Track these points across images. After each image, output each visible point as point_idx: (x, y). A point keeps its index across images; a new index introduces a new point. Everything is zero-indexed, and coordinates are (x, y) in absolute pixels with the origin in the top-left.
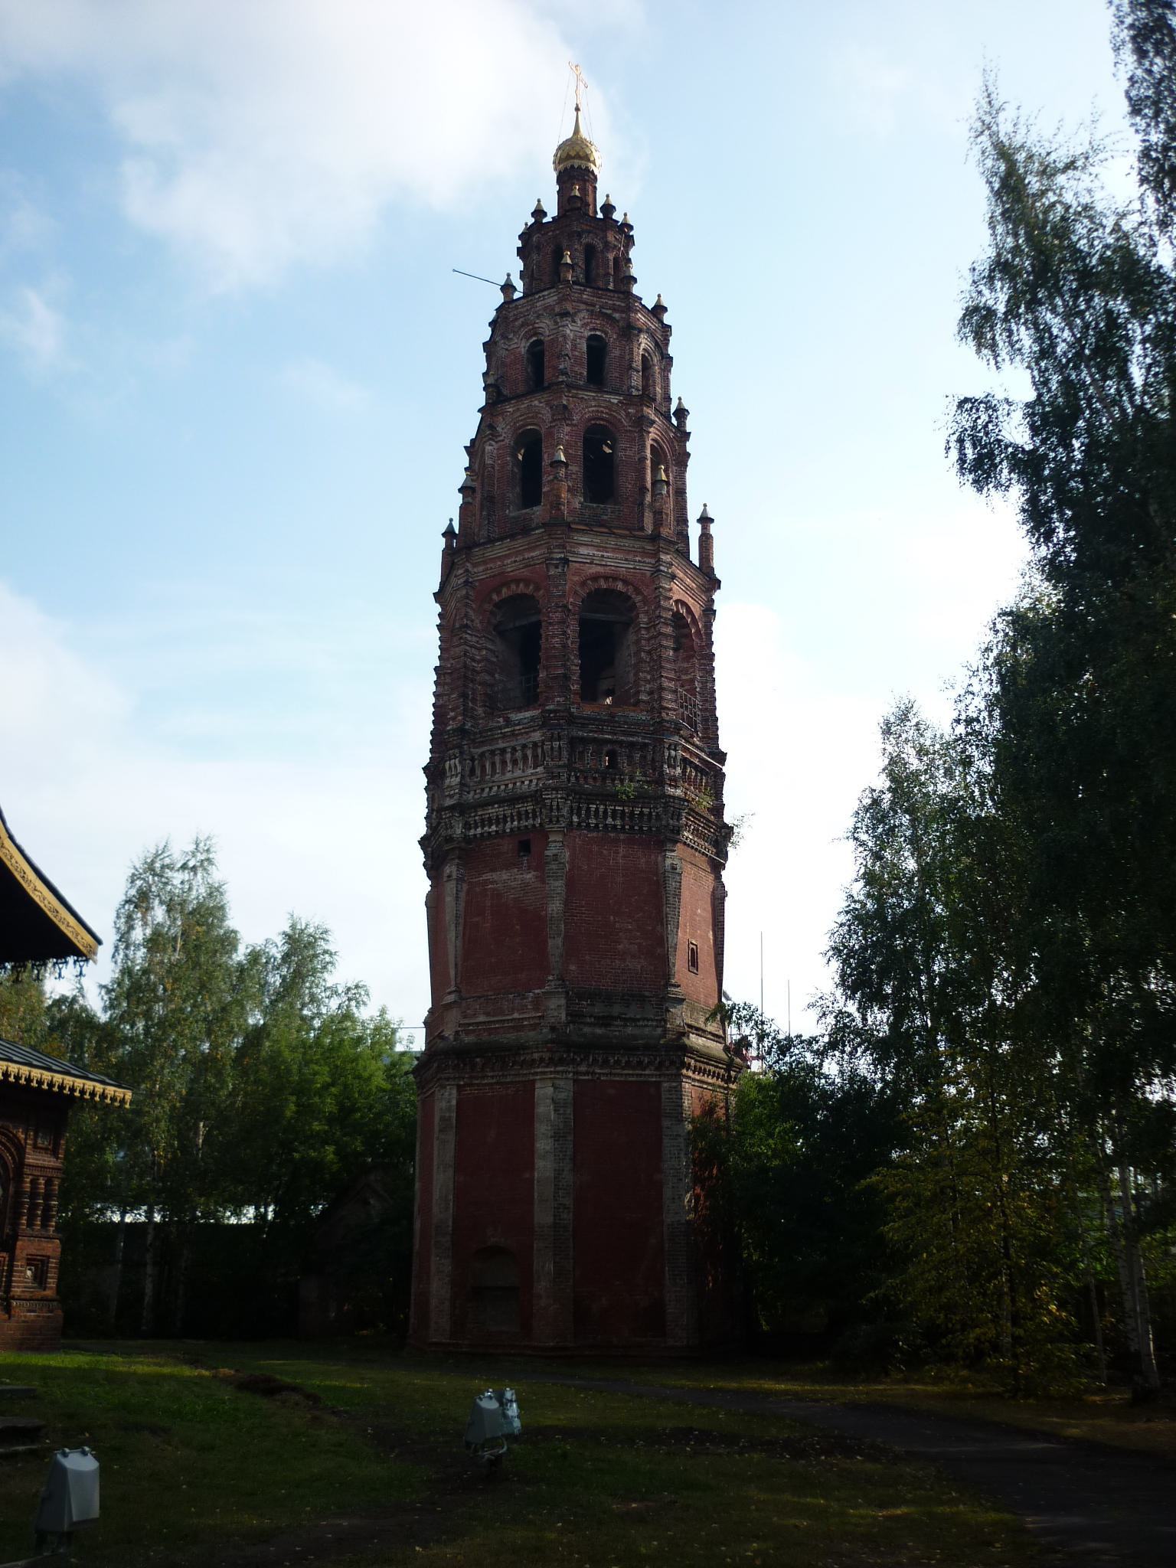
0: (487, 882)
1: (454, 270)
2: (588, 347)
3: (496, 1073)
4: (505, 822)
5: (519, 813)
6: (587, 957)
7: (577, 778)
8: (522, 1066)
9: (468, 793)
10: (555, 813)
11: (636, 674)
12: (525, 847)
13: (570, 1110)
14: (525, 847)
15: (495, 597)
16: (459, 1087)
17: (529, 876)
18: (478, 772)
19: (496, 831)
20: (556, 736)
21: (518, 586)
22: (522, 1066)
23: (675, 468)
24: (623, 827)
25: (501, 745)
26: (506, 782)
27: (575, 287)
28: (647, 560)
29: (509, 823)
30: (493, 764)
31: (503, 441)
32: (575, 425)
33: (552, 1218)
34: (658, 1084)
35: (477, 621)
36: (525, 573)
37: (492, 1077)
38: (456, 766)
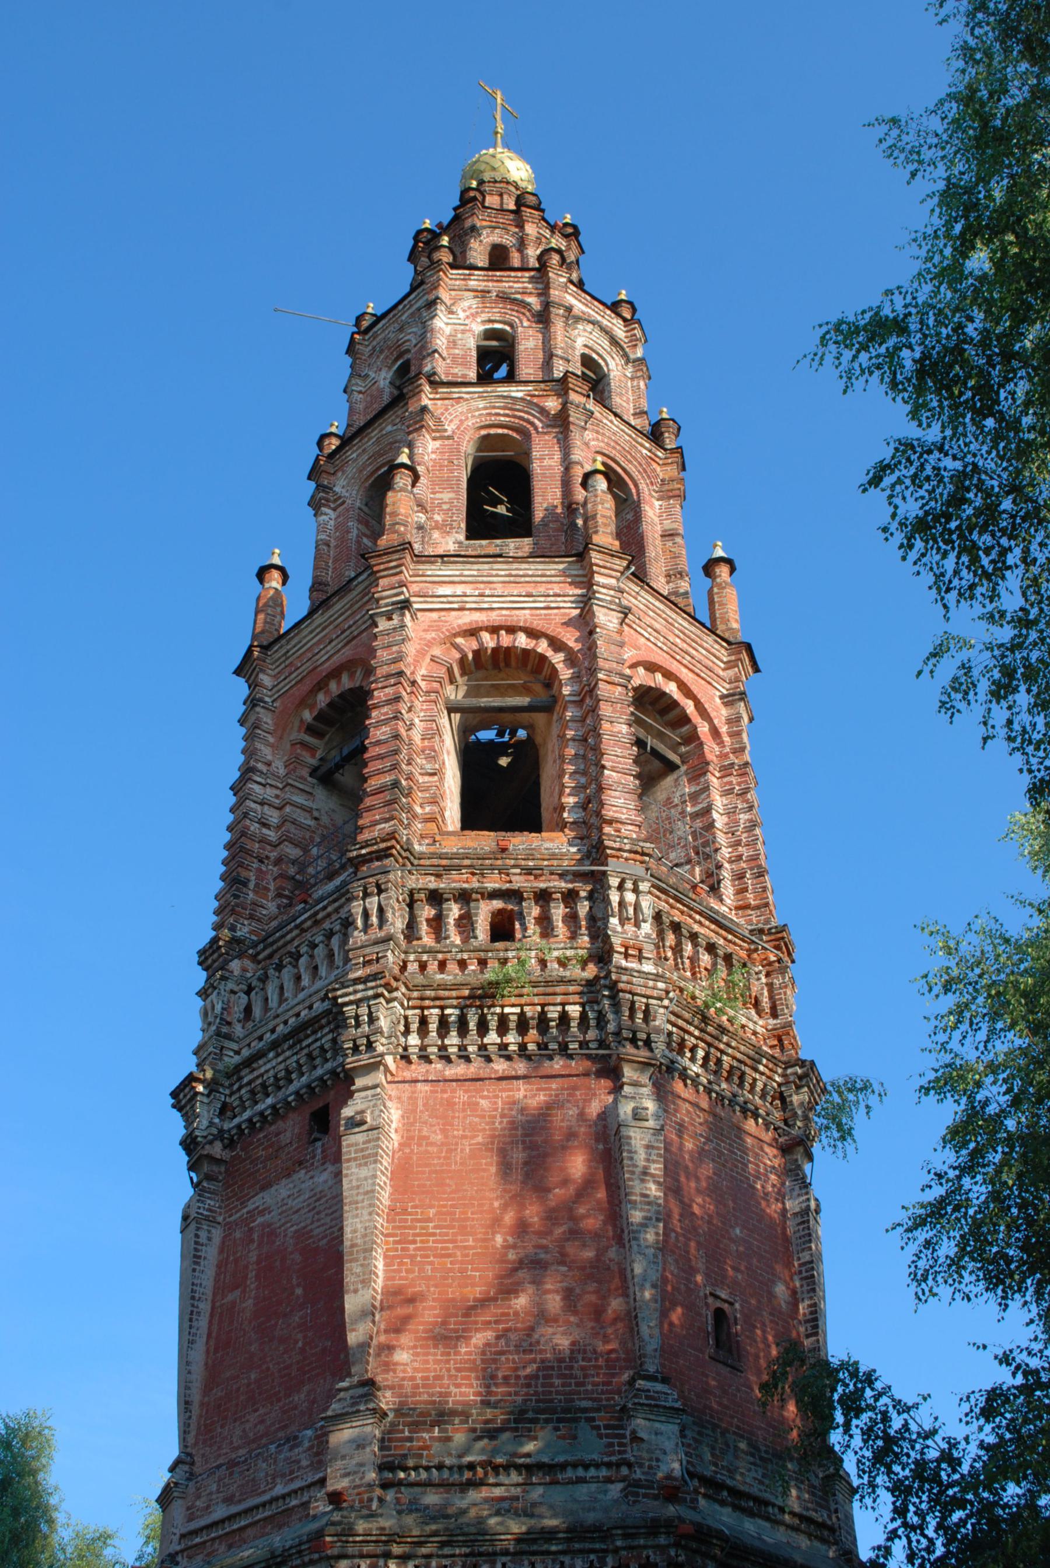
23: (657, 504)
24: (523, 1047)
26: (296, 1010)
32: (449, 438)
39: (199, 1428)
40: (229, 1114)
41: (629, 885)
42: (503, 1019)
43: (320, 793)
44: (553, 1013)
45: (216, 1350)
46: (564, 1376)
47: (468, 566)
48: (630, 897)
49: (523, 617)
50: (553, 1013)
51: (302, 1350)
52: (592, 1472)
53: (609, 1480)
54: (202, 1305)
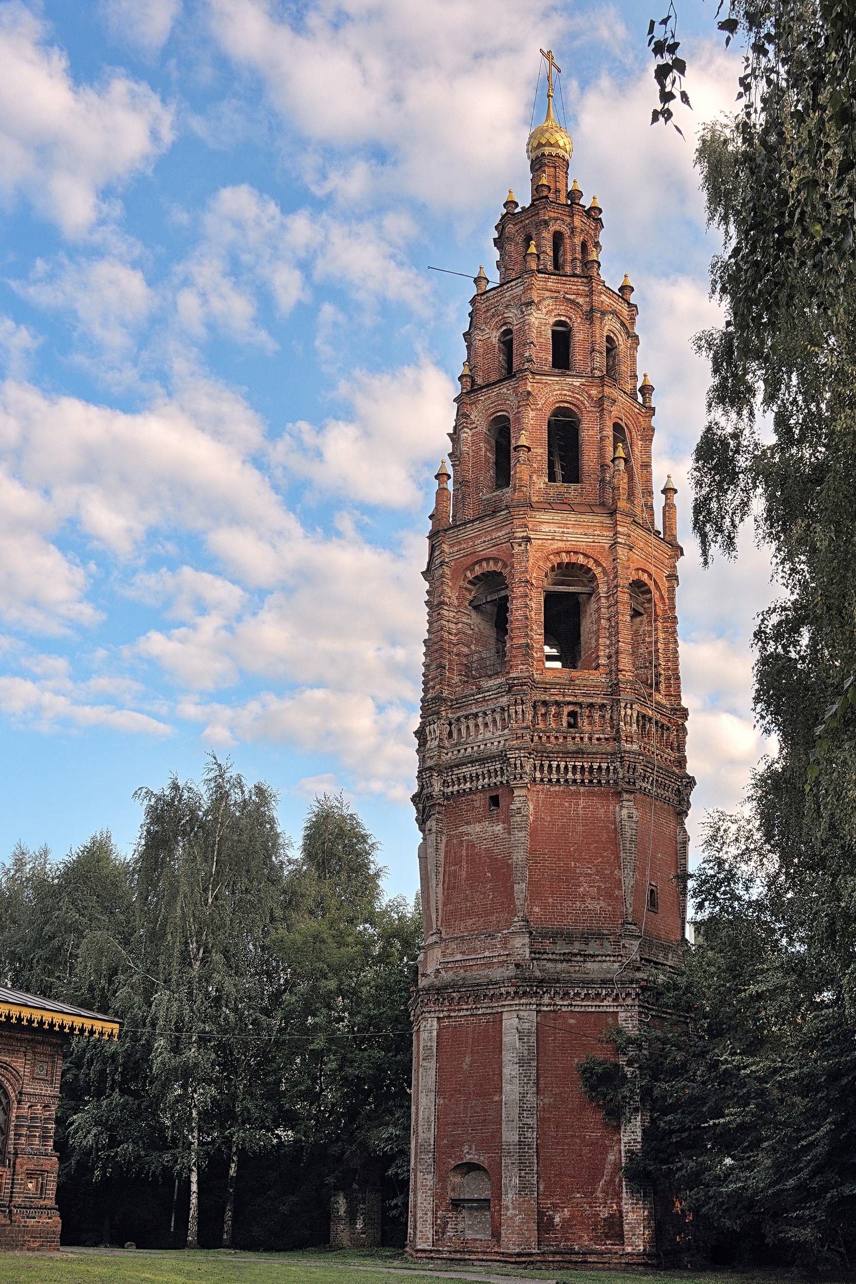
1: (429, 267)
2: (554, 332)
3: (470, 1007)
4: (478, 779)
5: (489, 771)
6: (550, 900)
7: (540, 738)
8: (492, 1000)
9: (447, 754)
10: (519, 770)
11: (597, 640)
13: (533, 1039)
14: (495, 801)
15: (468, 574)
16: (438, 1018)
17: (499, 828)
18: (455, 735)
19: (470, 789)
20: (519, 701)
21: (488, 563)
22: (492, 1000)
23: (640, 443)
24: (583, 781)
25: (475, 711)
26: (479, 744)
27: (540, 275)
28: (606, 534)
29: (481, 780)
30: (468, 727)
31: (476, 427)
32: (540, 410)
33: (518, 1137)
35: (454, 597)
36: (492, 552)
37: (467, 1010)
38: (434, 731)
39: (442, 920)
40: (446, 784)
41: (629, 706)
42: (574, 767)
43: (473, 614)
44: (596, 766)
45: (448, 889)
46: (597, 920)
47: (557, 515)
48: (629, 712)
49: (582, 546)
50: (596, 766)
51: (492, 900)
52: (608, 958)
53: (614, 962)
54: (440, 869)
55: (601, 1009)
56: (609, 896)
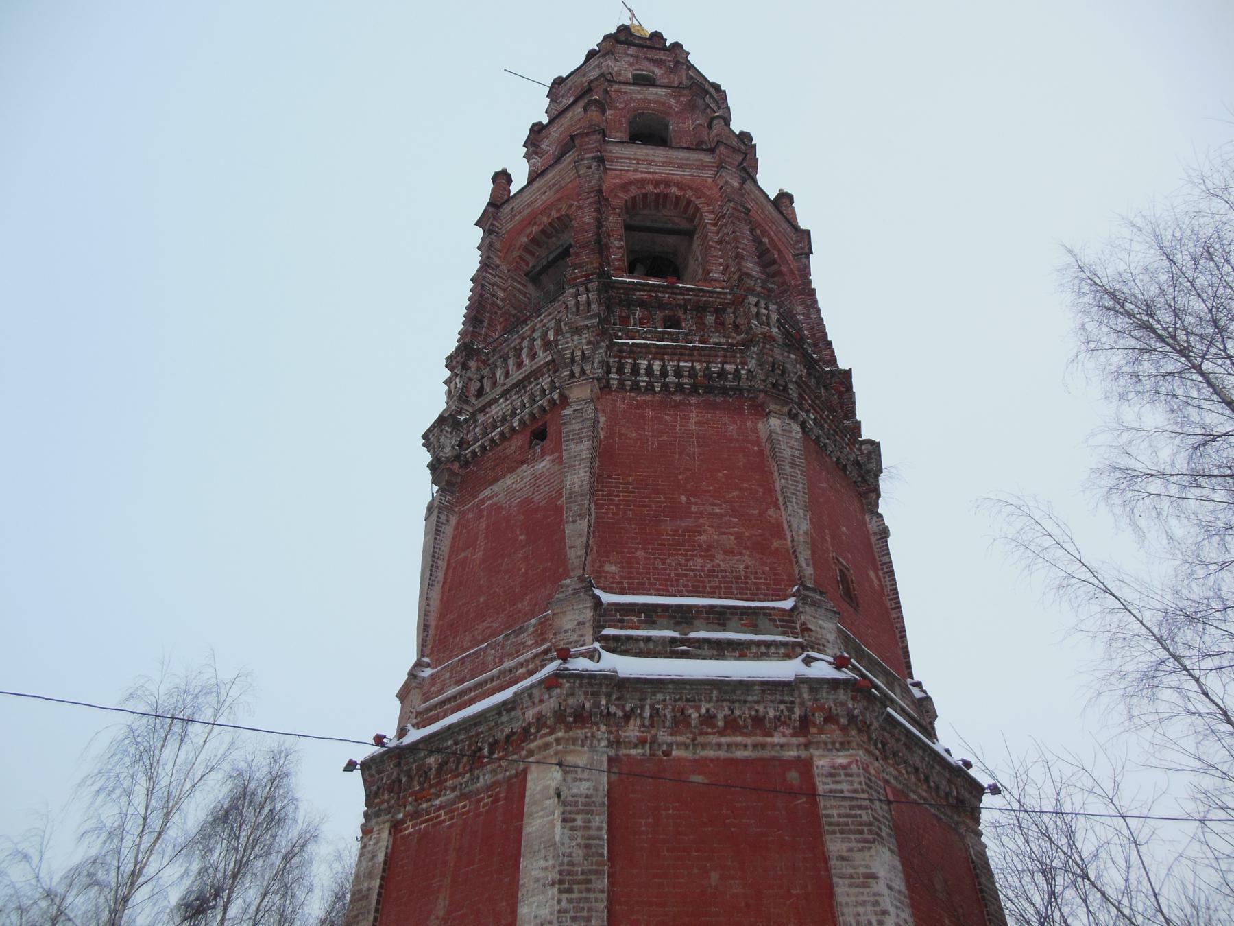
0: (482, 502)
1: (505, 70)
12: (540, 435)
13: (600, 821)
34: (805, 766)
39: (434, 642)
40: (465, 446)
45: (450, 590)
51: (526, 573)
54: (440, 562)
55: (767, 754)
56: (760, 547)
